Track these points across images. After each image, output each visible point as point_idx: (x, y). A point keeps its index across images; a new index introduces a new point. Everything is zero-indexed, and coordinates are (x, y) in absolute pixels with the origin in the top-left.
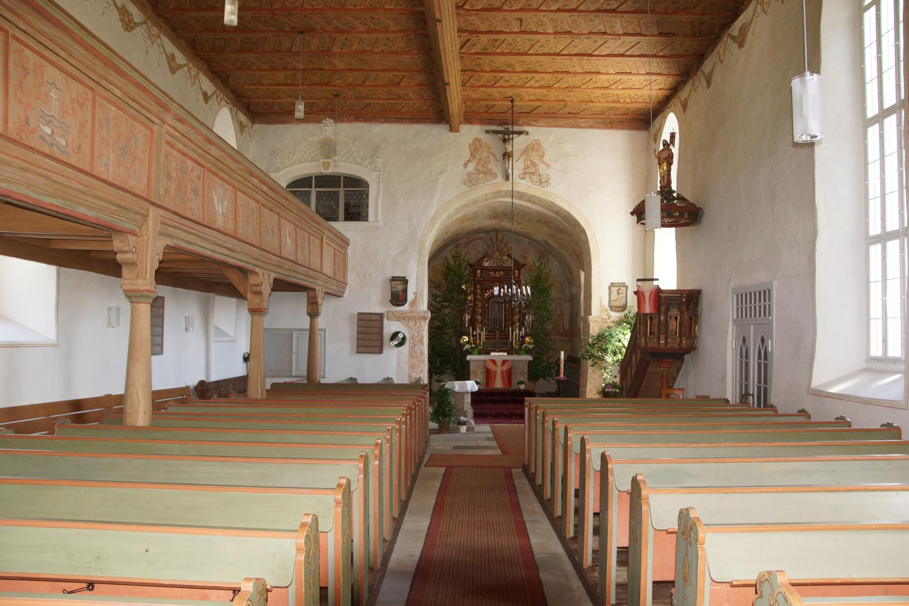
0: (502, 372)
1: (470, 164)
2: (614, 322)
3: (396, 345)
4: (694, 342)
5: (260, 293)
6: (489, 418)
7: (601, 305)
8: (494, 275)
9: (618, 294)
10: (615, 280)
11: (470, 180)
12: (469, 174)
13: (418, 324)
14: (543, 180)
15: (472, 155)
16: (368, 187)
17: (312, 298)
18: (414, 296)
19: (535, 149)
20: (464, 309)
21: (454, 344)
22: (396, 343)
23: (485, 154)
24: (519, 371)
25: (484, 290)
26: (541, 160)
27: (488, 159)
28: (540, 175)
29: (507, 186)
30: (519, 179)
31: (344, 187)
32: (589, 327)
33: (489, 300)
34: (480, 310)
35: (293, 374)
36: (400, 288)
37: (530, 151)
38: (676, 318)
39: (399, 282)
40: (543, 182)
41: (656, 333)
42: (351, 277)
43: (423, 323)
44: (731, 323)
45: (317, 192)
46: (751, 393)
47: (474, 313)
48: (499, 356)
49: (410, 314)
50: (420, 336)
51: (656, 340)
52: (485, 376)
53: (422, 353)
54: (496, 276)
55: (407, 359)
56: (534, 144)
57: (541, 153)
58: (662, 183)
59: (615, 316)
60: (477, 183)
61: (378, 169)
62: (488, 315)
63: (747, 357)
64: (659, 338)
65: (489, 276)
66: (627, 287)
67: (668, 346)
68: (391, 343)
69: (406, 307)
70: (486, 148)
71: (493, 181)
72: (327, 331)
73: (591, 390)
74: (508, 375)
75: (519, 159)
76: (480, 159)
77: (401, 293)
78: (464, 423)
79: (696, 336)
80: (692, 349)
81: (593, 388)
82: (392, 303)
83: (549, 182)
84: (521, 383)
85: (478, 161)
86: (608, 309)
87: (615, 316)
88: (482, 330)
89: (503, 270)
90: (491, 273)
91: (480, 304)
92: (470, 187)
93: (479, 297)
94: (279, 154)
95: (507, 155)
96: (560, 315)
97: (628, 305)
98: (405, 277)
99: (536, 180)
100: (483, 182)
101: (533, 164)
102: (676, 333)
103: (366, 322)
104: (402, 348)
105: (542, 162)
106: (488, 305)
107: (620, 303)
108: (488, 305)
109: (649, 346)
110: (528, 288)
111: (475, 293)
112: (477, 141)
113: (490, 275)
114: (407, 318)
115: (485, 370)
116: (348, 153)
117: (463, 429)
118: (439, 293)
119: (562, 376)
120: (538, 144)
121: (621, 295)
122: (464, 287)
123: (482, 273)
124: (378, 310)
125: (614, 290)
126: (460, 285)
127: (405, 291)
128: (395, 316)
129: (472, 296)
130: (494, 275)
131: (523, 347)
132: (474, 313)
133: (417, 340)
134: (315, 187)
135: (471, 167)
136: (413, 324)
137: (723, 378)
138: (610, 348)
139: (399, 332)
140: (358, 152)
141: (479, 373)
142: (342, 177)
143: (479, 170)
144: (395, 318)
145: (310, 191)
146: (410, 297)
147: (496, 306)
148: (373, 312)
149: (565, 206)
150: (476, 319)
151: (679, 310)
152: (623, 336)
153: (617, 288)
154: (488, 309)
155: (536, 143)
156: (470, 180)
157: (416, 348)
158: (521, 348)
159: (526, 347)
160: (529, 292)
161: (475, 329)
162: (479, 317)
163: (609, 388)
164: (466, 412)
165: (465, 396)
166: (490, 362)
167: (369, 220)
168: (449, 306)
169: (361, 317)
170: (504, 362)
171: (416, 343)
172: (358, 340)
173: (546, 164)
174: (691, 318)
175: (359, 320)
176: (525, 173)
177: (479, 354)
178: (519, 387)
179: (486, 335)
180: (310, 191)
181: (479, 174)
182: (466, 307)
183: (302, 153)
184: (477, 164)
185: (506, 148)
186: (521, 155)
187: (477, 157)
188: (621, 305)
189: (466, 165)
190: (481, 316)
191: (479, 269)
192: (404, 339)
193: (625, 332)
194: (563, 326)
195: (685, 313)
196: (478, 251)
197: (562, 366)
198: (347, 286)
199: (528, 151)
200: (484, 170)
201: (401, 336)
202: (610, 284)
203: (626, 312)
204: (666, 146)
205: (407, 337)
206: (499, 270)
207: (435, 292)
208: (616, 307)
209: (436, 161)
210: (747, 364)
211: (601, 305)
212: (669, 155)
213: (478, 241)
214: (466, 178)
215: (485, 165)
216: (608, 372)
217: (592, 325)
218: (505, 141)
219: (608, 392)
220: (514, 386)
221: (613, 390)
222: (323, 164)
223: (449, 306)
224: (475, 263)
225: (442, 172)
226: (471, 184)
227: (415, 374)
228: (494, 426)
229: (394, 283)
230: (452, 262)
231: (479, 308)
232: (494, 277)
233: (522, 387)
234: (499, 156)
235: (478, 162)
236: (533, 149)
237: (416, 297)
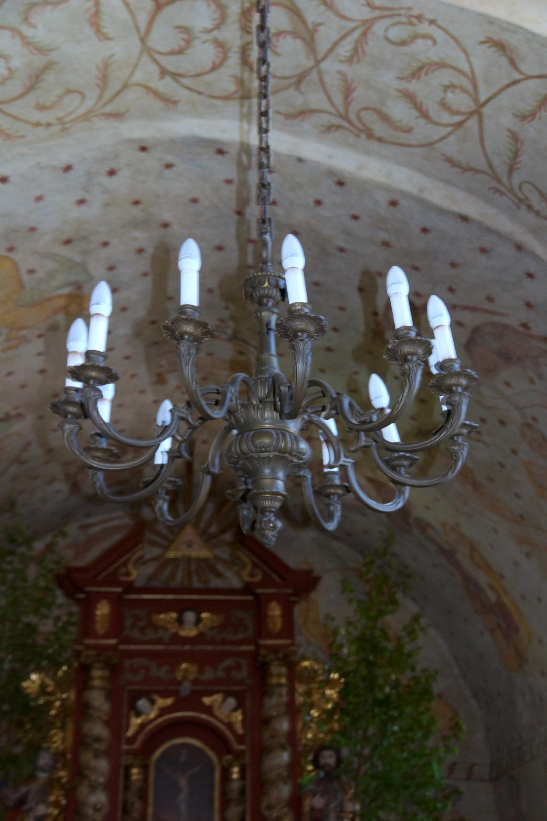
91: (103, 765)
108: (145, 768)
113: (156, 627)
147: (183, 782)
154: (143, 795)
182: (34, 787)
231: (93, 788)
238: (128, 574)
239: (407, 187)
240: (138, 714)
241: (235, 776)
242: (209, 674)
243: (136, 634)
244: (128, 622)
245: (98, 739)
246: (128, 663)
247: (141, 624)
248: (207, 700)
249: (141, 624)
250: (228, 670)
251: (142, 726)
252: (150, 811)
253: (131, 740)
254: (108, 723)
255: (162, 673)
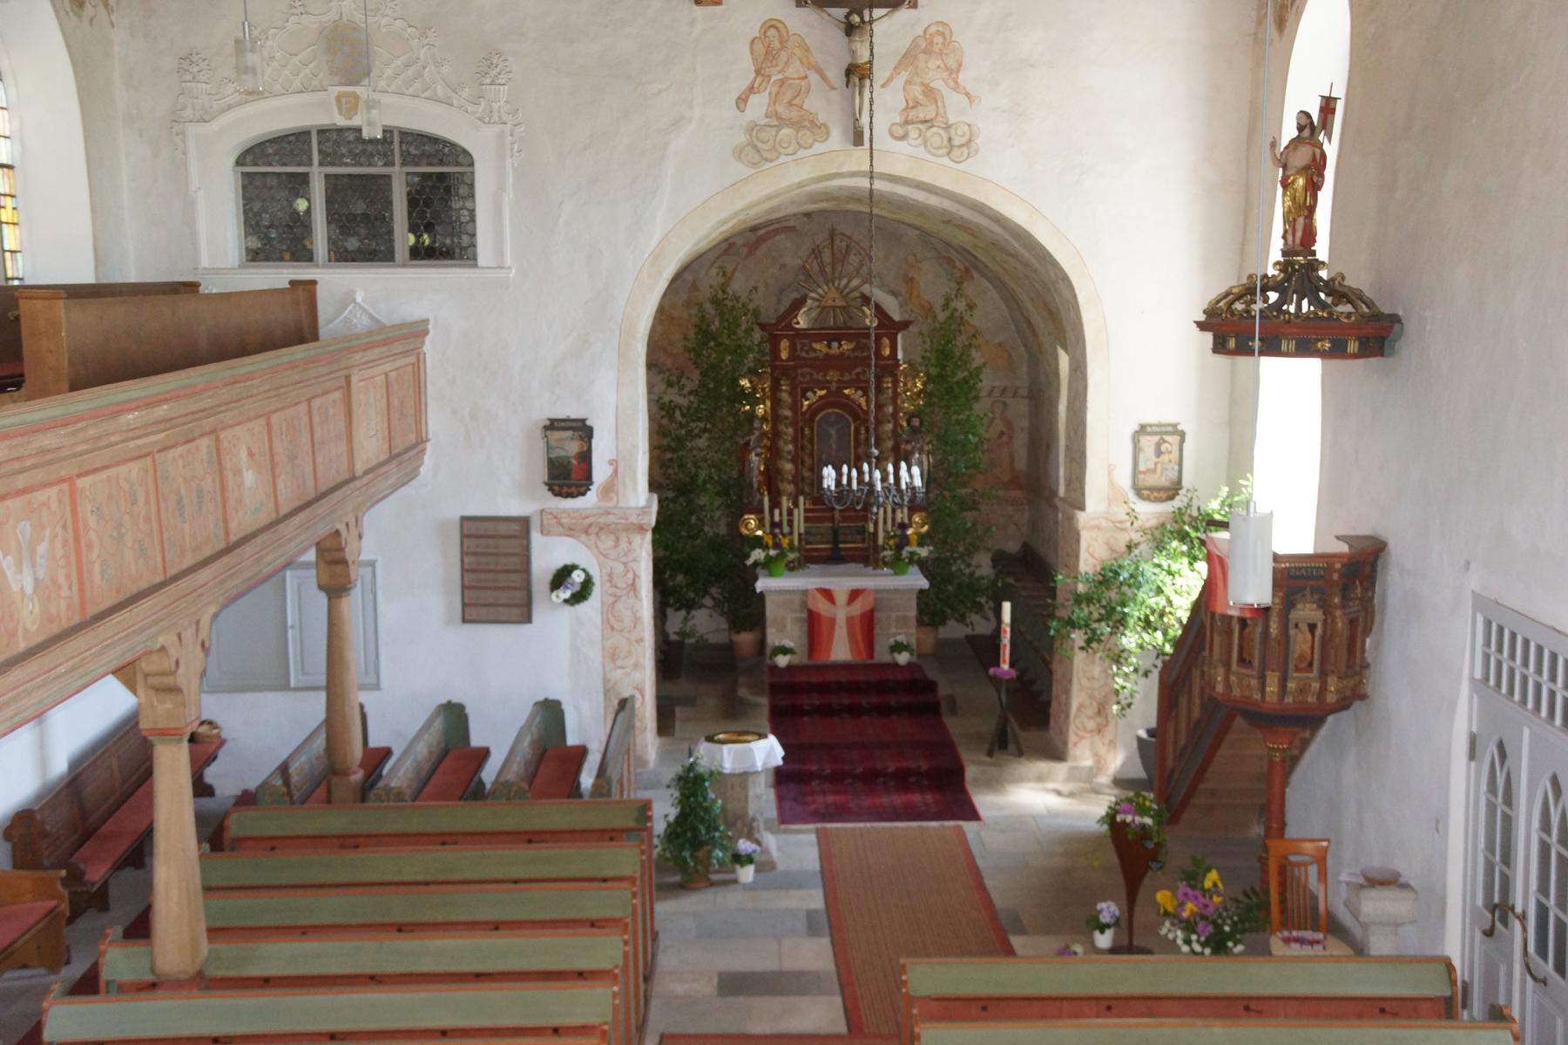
0: (850, 621)
1: (754, 99)
2: (1144, 532)
3: (566, 601)
4: (1361, 682)
5: (175, 690)
6: (815, 784)
7: (1112, 482)
8: (825, 350)
9: (1159, 453)
10: (1150, 418)
11: (755, 147)
12: (752, 128)
13: (624, 545)
14: (957, 141)
15: (758, 72)
16: (472, 164)
17: (329, 550)
18: (610, 470)
19: (936, 49)
20: (748, 443)
21: (723, 530)
22: (567, 594)
23: (794, 70)
24: (893, 615)
25: (799, 392)
26: (951, 83)
27: (803, 83)
28: (947, 127)
29: (857, 160)
30: (889, 139)
31: (404, 164)
32: (1078, 541)
33: (814, 414)
34: (790, 447)
35: (293, 684)
36: (572, 448)
37: (922, 57)
38: (1312, 627)
39: (569, 433)
40: (958, 145)
41: (1256, 663)
42: (437, 422)
43: (637, 539)
44: (1465, 687)
45: (327, 176)
46: (1519, 909)
47: (774, 453)
48: (842, 581)
49: (603, 520)
50: (630, 576)
51: (1254, 682)
52: (805, 628)
53: (637, 620)
54: (832, 352)
55: (597, 635)
56: (931, 35)
57: (951, 63)
58: (1290, 238)
59: (1150, 512)
60: (774, 155)
61: (496, 118)
62: (812, 455)
63: (1509, 799)
64: (1262, 679)
65: (812, 355)
66: (1182, 435)
67: (1289, 700)
68: (554, 596)
69: (590, 500)
70: (797, 51)
71: (819, 147)
72: (379, 567)
73: (1081, 707)
74: (867, 626)
75: (890, 80)
76: (782, 82)
77: (574, 462)
78: (748, 859)
79: (1366, 666)
80: (1354, 696)
81: (1087, 702)
82: (551, 489)
83: (973, 146)
84: (898, 648)
85: (774, 89)
86: (1131, 496)
87: (1150, 512)
88: (796, 504)
89: (849, 338)
90: (816, 346)
91: (790, 430)
92: (754, 164)
93: (787, 413)
94: (203, 65)
95: (857, 74)
96: (1002, 433)
97: (1186, 483)
98: (583, 421)
99: (936, 141)
100: (790, 150)
101: (930, 93)
102: (1311, 664)
103: (483, 542)
104: (582, 607)
105: (957, 87)
106: (812, 429)
107: (1163, 479)
109: (1236, 693)
110: (916, 470)
111: (776, 403)
112: (772, 32)
113: (815, 351)
114: (593, 530)
115: (805, 615)
116: (407, 66)
117: (747, 874)
118: (684, 402)
119: (1006, 667)
120: (943, 34)
121: (1165, 458)
122: (745, 383)
123: (792, 349)
124: (513, 506)
125: (1148, 443)
126: (735, 381)
127: (586, 457)
128: (561, 525)
129: (768, 403)
130: (825, 350)
131: (905, 553)
132: (774, 453)
133: (621, 584)
134: (321, 164)
135: (758, 106)
136: (610, 543)
137: (1439, 824)
138: (1134, 612)
139: (574, 567)
140: (438, 64)
141: (789, 626)
142: (396, 135)
143: (777, 116)
144: (561, 530)
145: (306, 175)
146: (600, 471)
147: (833, 432)
148: (502, 513)
149: (1017, 214)
150: (779, 471)
151: (1319, 606)
152: (1168, 579)
153: (1156, 439)
154: (811, 440)
155: (939, 33)
156: (755, 147)
157: (619, 606)
158: (897, 558)
159: (912, 554)
160: (918, 482)
161: (775, 504)
162: (788, 467)
163: (1125, 812)
164: (754, 820)
165: (751, 780)
166: (819, 597)
167: (481, 261)
168: (705, 430)
169: (471, 528)
170: (855, 595)
171: (618, 592)
172: (464, 588)
173: (967, 94)
174: (1352, 623)
175: (464, 536)
176: (907, 122)
177: (792, 568)
178: (894, 658)
179: (806, 511)
180: (306, 175)
181: (779, 127)
182: (753, 438)
183: (275, 64)
184: (775, 99)
185: (853, 53)
186: (895, 69)
187: (773, 78)
188: (1167, 484)
189: (742, 101)
190: (793, 461)
191: (783, 336)
192: (587, 585)
193: (1175, 567)
194: (1012, 462)
195: (1338, 613)
196: (783, 266)
197: (1006, 640)
198: (429, 446)
199: (915, 57)
200: (794, 114)
201: (578, 577)
202: (1137, 428)
203: (1178, 503)
204: (1306, 133)
205: (596, 580)
206: (838, 338)
207: (673, 396)
208: (1152, 489)
209: (660, 92)
210: (1508, 821)
211: (1112, 482)
212: (1314, 159)
213: (781, 237)
214: (743, 138)
215: (796, 101)
216: (1126, 675)
217: (1086, 538)
218: (850, 30)
219: (1124, 822)
220: (882, 655)
221: (1138, 819)
222: (338, 99)
223: (705, 430)
224: (773, 321)
225: (678, 123)
226: (757, 159)
227: (619, 672)
228: (824, 829)
229: (556, 435)
230: (710, 309)
231: (786, 442)
232: (827, 354)
233: (903, 658)
234: (836, 74)
235: (777, 94)
236: (928, 51)
237: (616, 472)
238: (798, 323)
239: (950, 209)
240: (807, 399)
241: (863, 432)
242: (847, 377)
243: (804, 354)
244: (799, 347)
245: (787, 418)
246: (799, 371)
247: (806, 348)
248: (846, 392)
249: (806, 348)
250: (858, 374)
251: (810, 406)
252: (816, 447)
253: (803, 414)
254: (790, 409)
255: (820, 377)
